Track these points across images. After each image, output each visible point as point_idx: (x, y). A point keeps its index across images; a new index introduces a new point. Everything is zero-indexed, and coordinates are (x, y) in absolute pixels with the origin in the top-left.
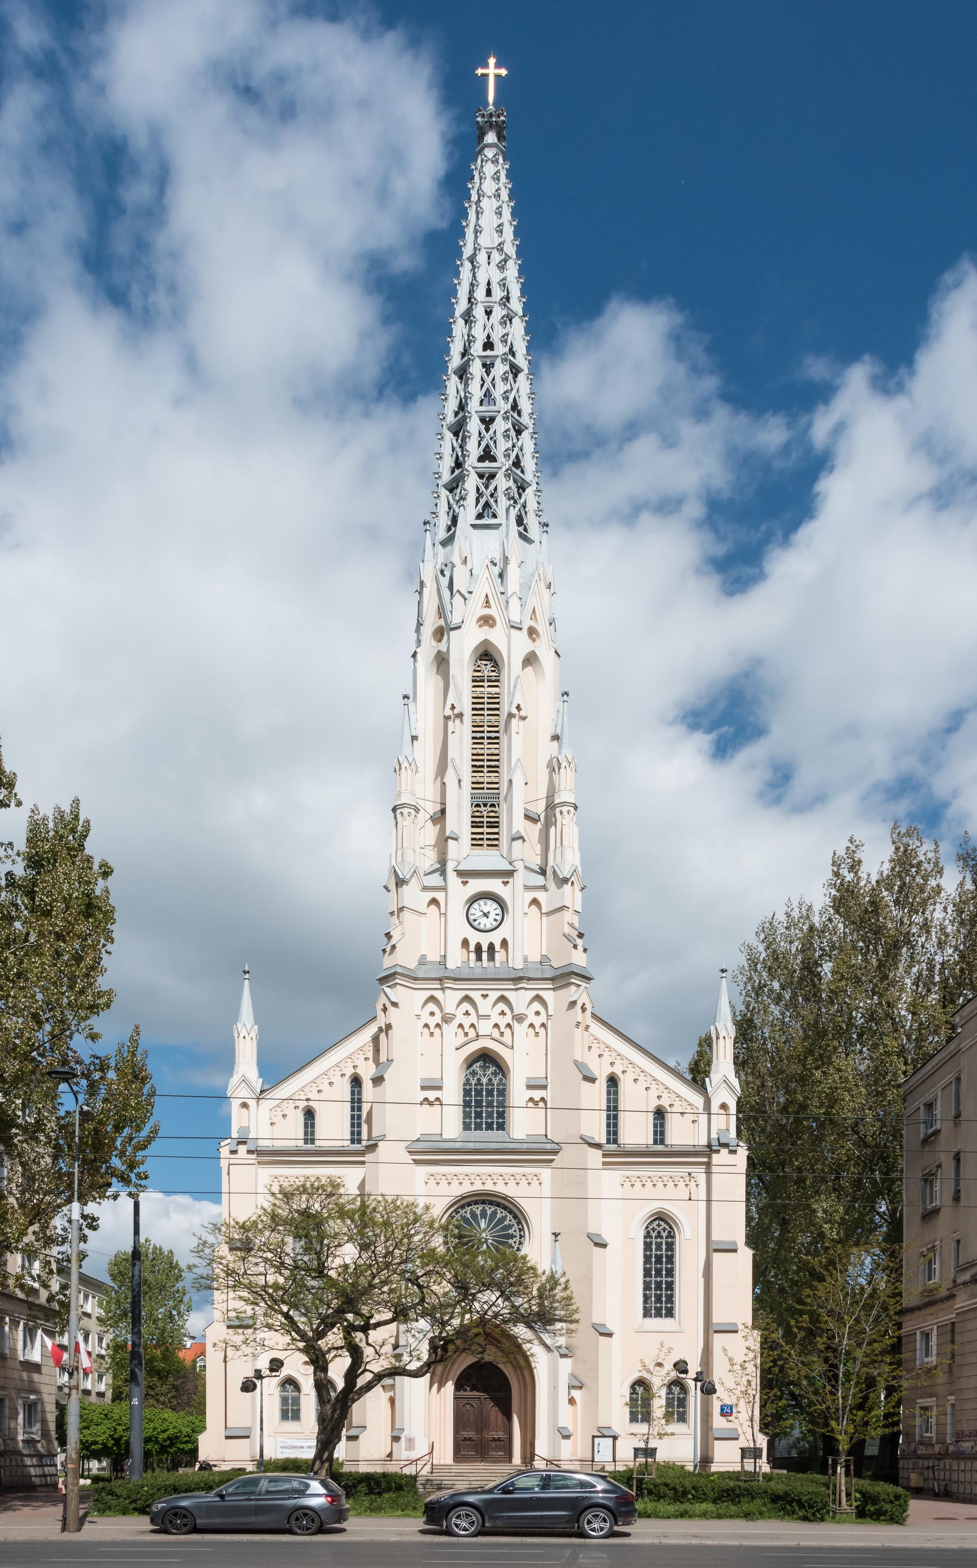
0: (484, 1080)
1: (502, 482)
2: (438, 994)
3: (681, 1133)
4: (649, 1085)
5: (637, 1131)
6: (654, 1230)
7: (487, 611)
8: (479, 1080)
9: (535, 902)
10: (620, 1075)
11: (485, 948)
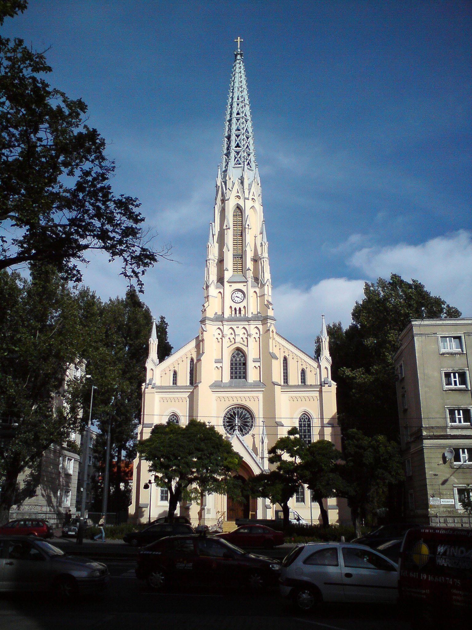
0: (238, 359)
1: (243, 154)
2: (221, 327)
3: (311, 379)
4: (299, 360)
5: (294, 379)
7: (238, 194)
9: (255, 292)
10: (288, 356)
11: (238, 309)
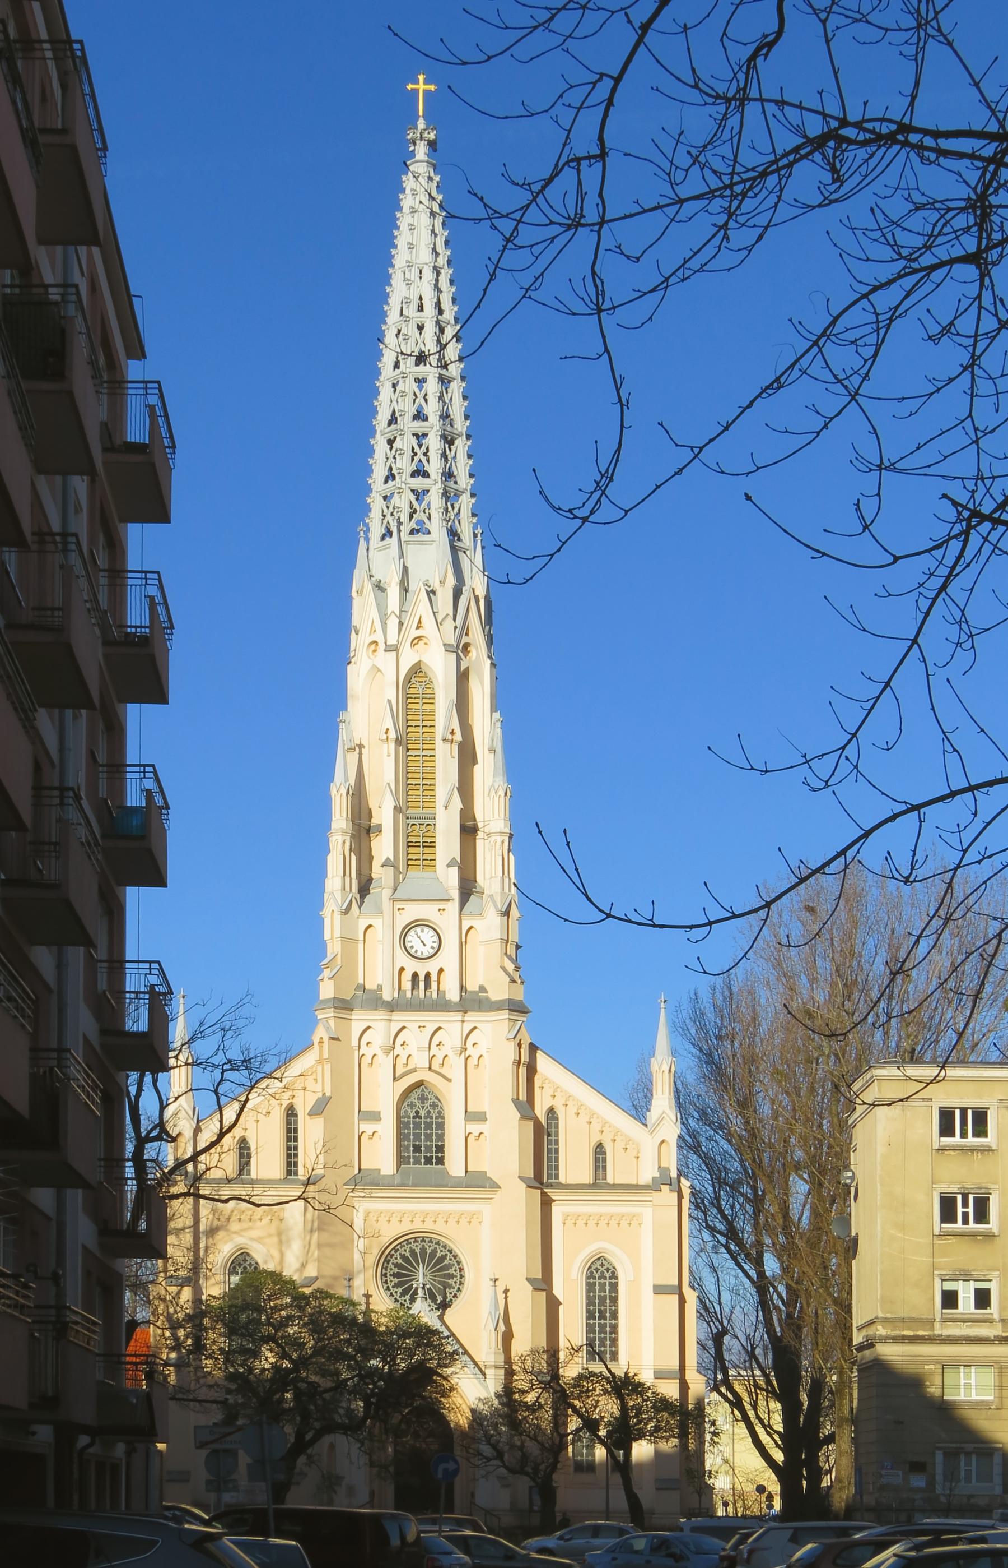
6: (597, 1270)
8: (417, 1112)
11: (422, 977)
